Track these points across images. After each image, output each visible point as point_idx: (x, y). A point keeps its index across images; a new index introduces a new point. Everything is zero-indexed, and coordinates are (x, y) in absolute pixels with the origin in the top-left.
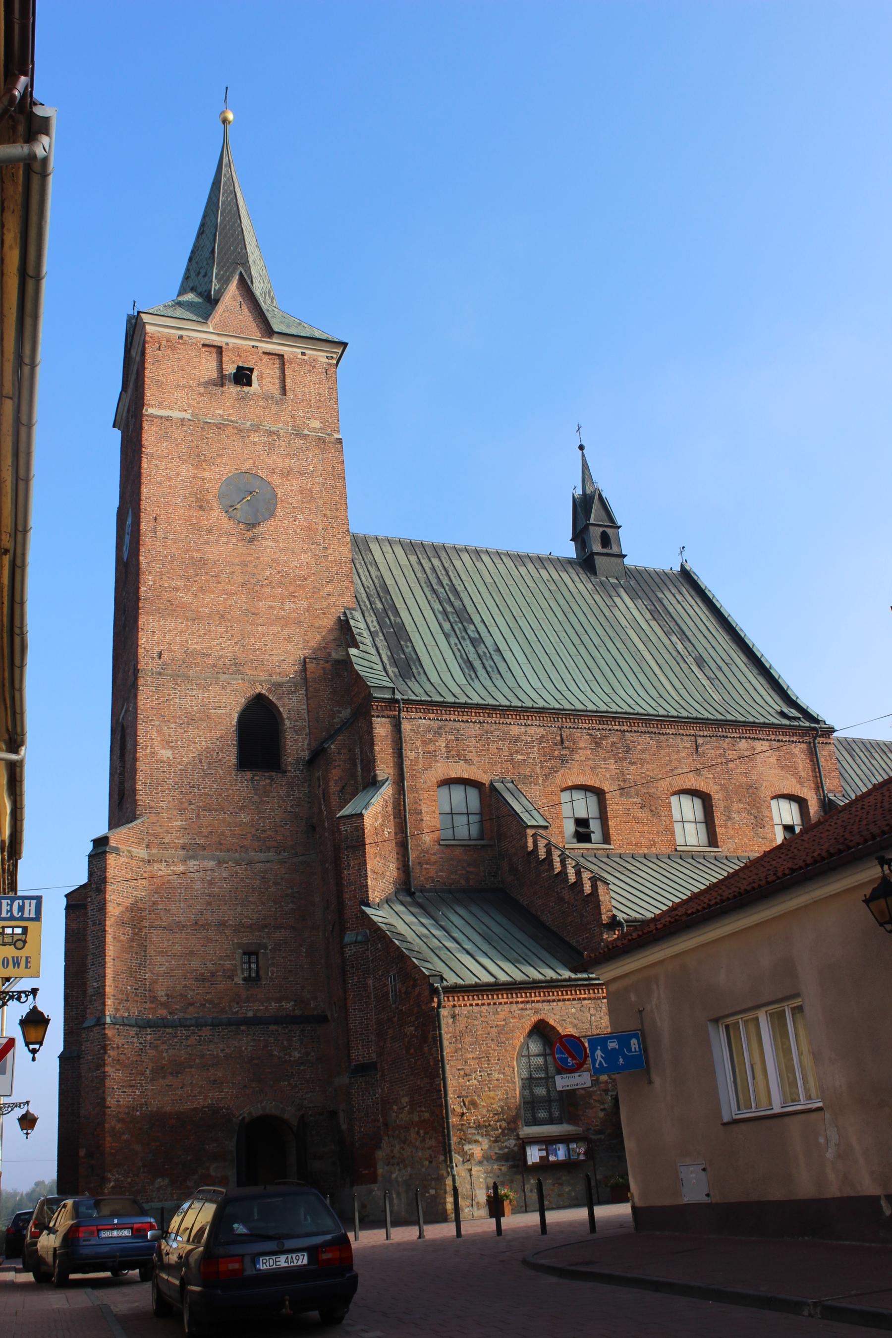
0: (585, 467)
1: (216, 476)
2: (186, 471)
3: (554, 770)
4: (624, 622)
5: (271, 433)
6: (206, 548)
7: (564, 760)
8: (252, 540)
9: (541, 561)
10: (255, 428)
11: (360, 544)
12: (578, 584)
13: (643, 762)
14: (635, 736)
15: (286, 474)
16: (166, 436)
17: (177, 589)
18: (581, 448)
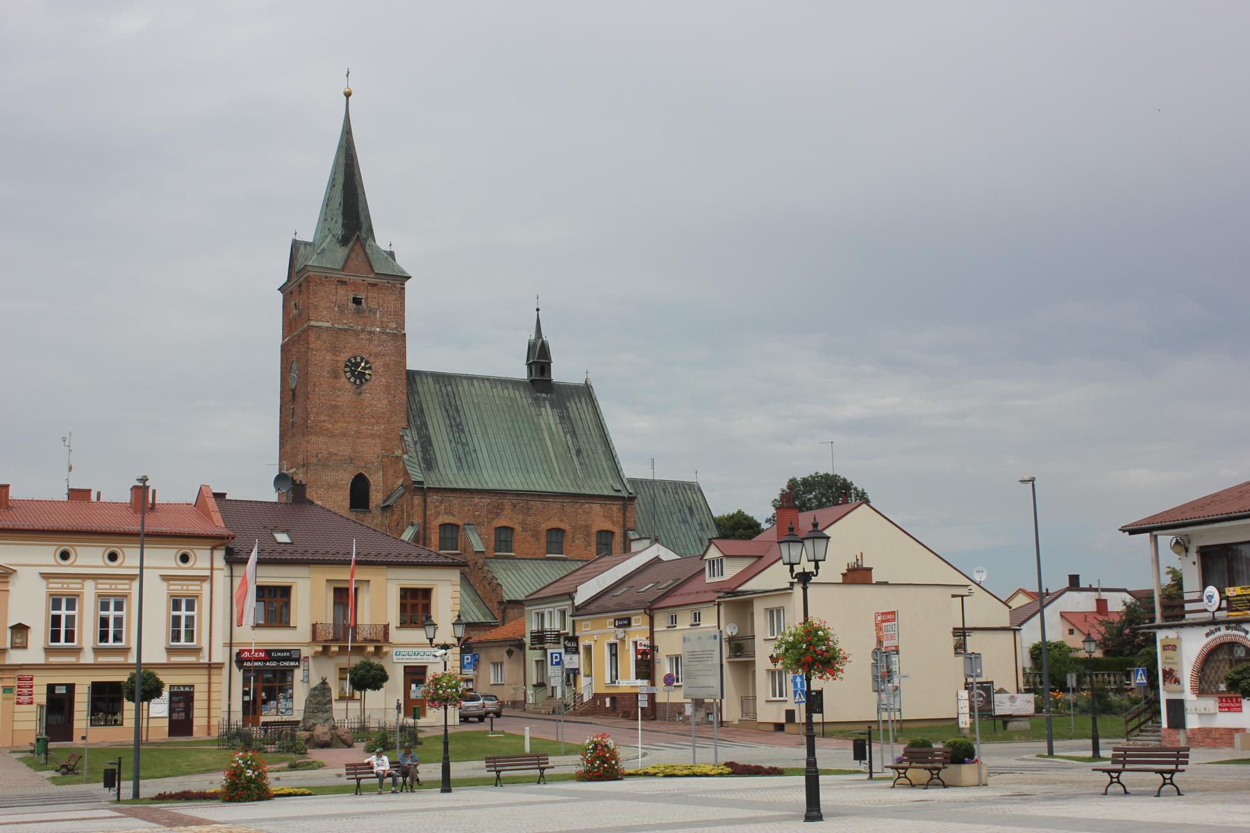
1: (343, 357)
2: (329, 356)
3: (493, 519)
4: (543, 426)
5: (370, 332)
7: (497, 514)
8: (360, 393)
9: (505, 382)
10: (363, 331)
11: (412, 376)
12: (524, 399)
15: (377, 356)
16: (319, 338)
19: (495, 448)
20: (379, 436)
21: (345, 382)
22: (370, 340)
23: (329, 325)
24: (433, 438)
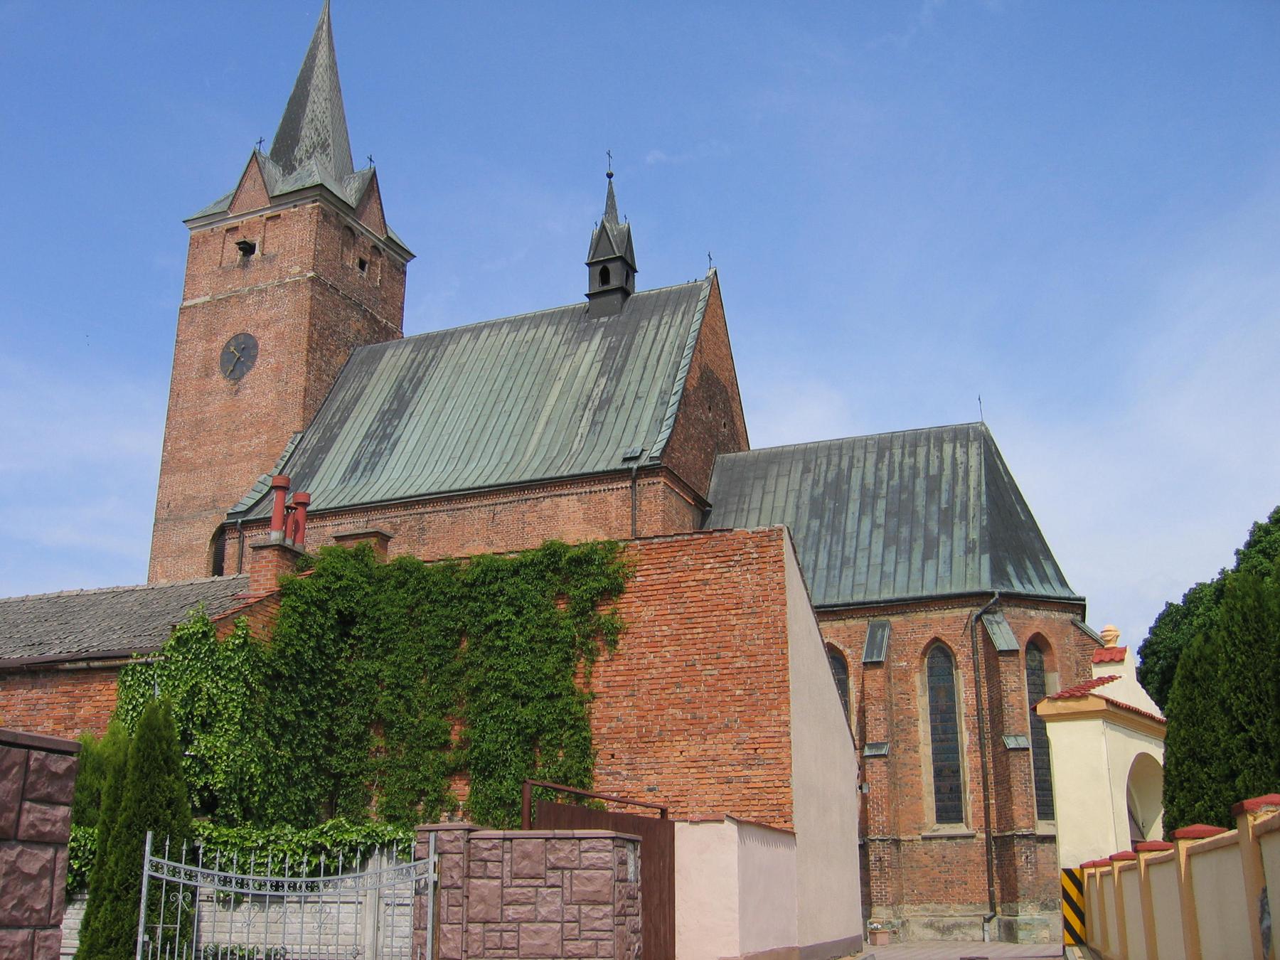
0: (611, 196)
2: (201, 346)
5: (261, 291)
6: (206, 409)
8: (237, 391)
10: (251, 292)
13: (435, 541)
14: (433, 516)
15: (266, 326)
17: (184, 449)
18: (610, 176)
19: (438, 430)
20: (258, 455)
21: (219, 380)
22: (261, 303)
23: (208, 298)
24: (340, 439)
